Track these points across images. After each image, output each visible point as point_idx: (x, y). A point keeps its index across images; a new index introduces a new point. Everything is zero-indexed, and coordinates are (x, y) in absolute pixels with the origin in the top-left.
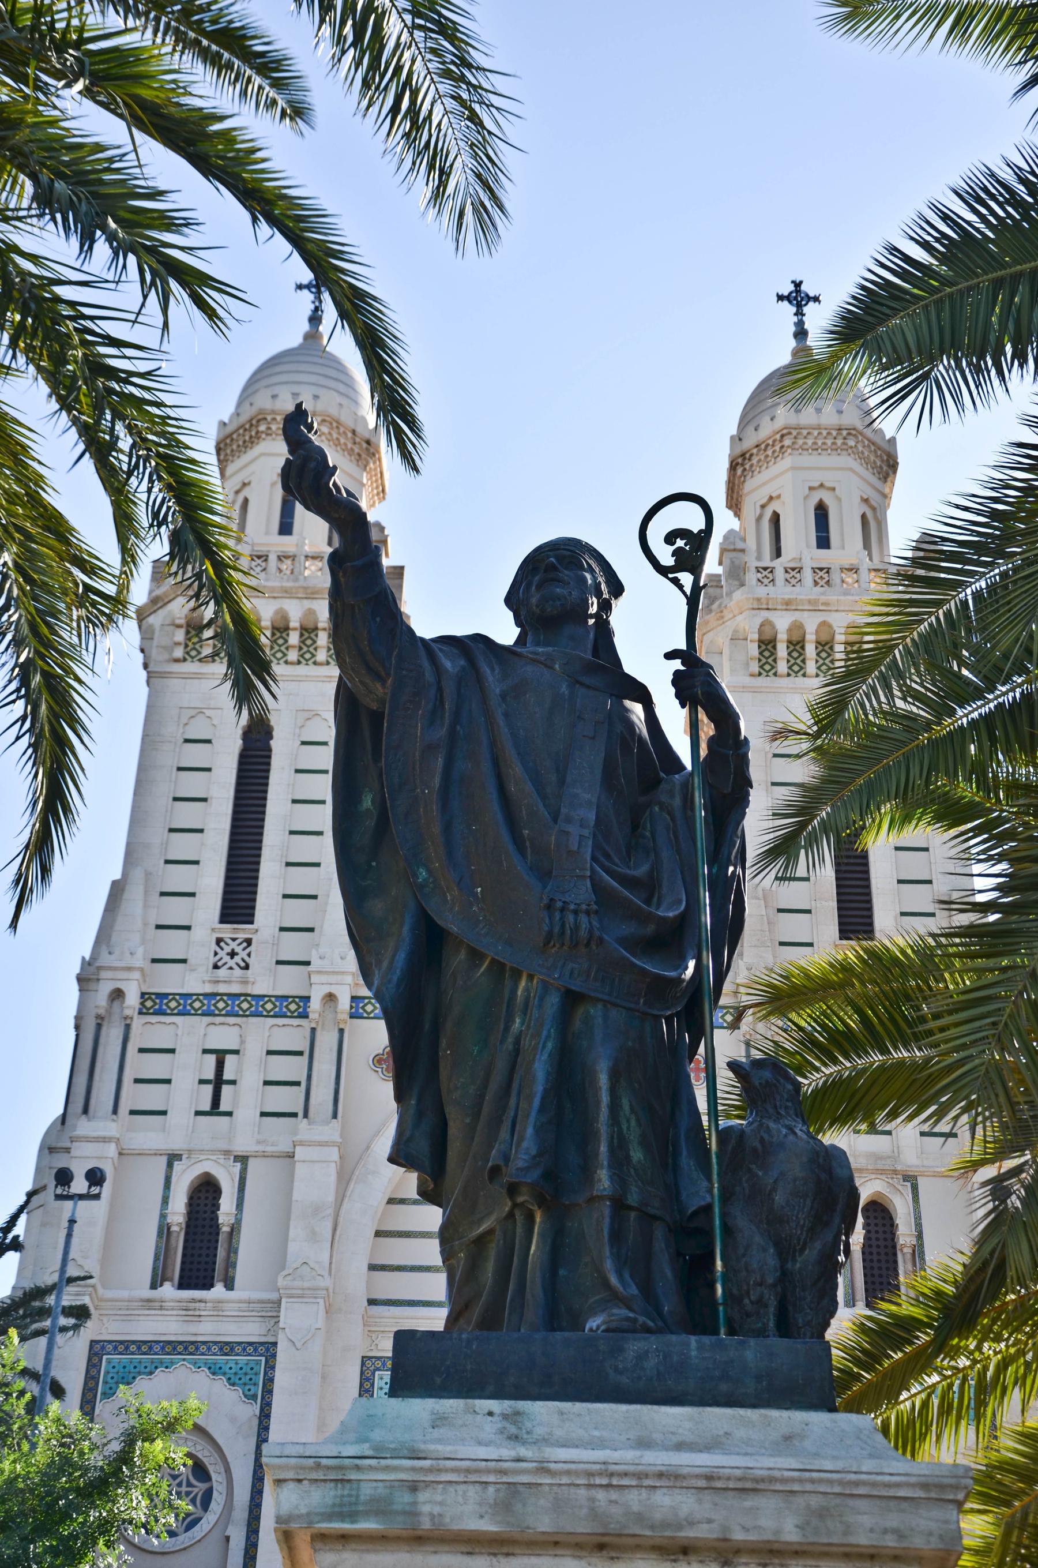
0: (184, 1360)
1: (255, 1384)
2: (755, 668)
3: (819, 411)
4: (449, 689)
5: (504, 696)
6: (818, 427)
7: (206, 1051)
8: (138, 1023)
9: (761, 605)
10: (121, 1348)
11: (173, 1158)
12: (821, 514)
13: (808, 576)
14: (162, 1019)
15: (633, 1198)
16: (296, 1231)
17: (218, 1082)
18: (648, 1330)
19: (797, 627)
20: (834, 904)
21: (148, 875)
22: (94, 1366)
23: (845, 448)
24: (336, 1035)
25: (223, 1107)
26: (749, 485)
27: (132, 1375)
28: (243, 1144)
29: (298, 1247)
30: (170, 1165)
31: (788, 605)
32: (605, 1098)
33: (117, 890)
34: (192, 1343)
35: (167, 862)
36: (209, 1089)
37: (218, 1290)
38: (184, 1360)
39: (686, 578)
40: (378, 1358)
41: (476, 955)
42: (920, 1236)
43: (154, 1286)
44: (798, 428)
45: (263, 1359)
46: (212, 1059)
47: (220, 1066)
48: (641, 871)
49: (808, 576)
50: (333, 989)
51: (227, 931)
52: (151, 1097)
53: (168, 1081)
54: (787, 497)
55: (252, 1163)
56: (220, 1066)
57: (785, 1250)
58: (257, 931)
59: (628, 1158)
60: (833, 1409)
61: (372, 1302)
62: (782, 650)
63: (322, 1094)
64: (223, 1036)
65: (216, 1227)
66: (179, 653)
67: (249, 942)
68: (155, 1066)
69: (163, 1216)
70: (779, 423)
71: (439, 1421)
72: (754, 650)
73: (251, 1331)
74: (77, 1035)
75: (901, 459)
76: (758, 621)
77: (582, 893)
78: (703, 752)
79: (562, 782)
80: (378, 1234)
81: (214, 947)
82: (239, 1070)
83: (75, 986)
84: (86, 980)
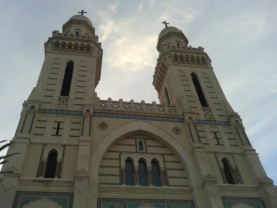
0: (45, 197)
1: (66, 204)
7: (55, 122)
8: (37, 115)
10: (26, 193)
11: (45, 145)
14: (44, 114)
17: (58, 128)
19: (181, 55)
22: (17, 198)
23: (181, 36)
24: (90, 118)
25: (59, 134)
27: (29, 201)
30: (44, 147)
34: (48, 192)
35: (48, 84)
36: (56, 130)
37: (56, 179)
38: (45, 197)
40: (102, 198)
42: (237, 167)
43: (37, 177)
45: (69, 197)
47: (59, 126)
50: (89, 109)
53: (45, 128)
56: (59, 126)
58: (69, 98)
61: (100, 184)
63: (86, 131)
64: (60, 119)
66: (53, 49)
67: (67, 100)
69: (41, 159)
73: (65, 190)
74: (21, 117)
81: (59, 100)
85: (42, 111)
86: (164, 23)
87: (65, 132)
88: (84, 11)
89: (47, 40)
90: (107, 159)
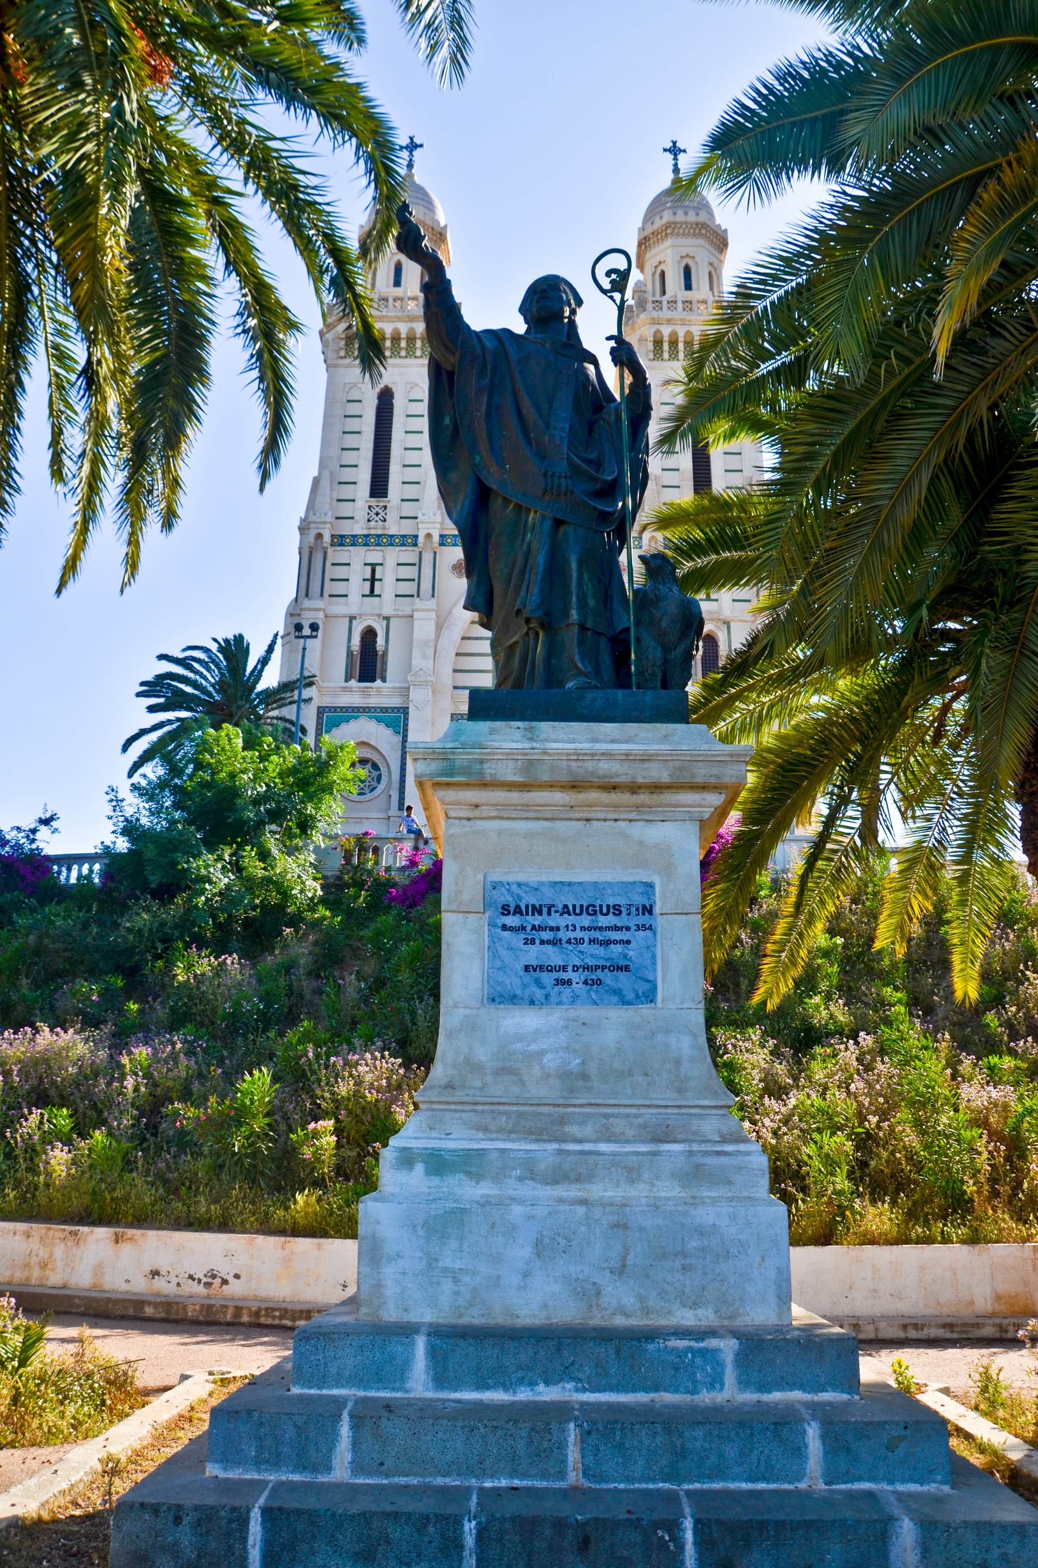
2: (651, 356)
3: (686, 214)
4: (489, 357)
5: (519, 362)
6: (686, 223)
8: (330, 550)
9: (655, 322)
11: (352, 618)
12: (687, 272)
13: (680, 305)
15: (589, 624)
16: (416, 653)
17: (373, 580)
18: (596, 687)
20: (692, 483)
21: (331, 473)
23: (700, 235)
26: (649, 255)
28: (387, 611)
29: (417, 661)
30: (351, 622)
31: (669, 322)
32: (575, 575)
33: (316, 482)
36: (368, 584)
39: (617, 296)
41: (506, 501)
43: (346, 681)
44: (675, 223)
46: (369, 569)
47: (373, 571)
48: (593, 456)
49: (680, 305)
50: (431, 531)
51: (373, 502)
52: (339, 588)
54: (669, 261)
55: (392, 620)
56: (373, 571)
57: (666, 649)
59: (587, 604)
60: (688, 723)
61: (455, 688)
62: (666, 346)
63: (426, 585)
65: (375, 652)
67: (385, 507)
68: (340, 572)
69: (349, 647)
70: (665, 220)
71: (492, 731)
72: (651, 346)
73: (395, 702)
75: (730, 241)
76: (653, 330)
77: (563, 467)
78: (627, 391)
79: (551, 408)
80: (457, 654)
82: (383, 574)
83: (297, 532)
84: (303, 529)
85: (339, 540)
86: (669, 150)
87: (387, 587)
88: (417, 141)
89: (322, 357)
90: (469, 638)
